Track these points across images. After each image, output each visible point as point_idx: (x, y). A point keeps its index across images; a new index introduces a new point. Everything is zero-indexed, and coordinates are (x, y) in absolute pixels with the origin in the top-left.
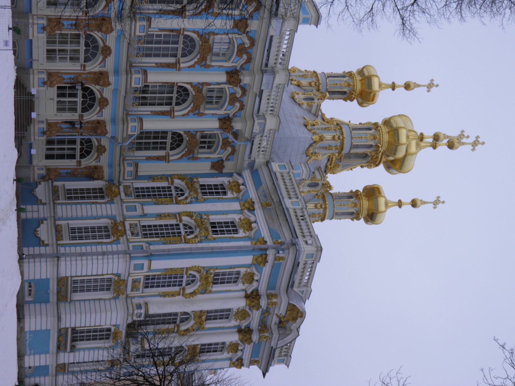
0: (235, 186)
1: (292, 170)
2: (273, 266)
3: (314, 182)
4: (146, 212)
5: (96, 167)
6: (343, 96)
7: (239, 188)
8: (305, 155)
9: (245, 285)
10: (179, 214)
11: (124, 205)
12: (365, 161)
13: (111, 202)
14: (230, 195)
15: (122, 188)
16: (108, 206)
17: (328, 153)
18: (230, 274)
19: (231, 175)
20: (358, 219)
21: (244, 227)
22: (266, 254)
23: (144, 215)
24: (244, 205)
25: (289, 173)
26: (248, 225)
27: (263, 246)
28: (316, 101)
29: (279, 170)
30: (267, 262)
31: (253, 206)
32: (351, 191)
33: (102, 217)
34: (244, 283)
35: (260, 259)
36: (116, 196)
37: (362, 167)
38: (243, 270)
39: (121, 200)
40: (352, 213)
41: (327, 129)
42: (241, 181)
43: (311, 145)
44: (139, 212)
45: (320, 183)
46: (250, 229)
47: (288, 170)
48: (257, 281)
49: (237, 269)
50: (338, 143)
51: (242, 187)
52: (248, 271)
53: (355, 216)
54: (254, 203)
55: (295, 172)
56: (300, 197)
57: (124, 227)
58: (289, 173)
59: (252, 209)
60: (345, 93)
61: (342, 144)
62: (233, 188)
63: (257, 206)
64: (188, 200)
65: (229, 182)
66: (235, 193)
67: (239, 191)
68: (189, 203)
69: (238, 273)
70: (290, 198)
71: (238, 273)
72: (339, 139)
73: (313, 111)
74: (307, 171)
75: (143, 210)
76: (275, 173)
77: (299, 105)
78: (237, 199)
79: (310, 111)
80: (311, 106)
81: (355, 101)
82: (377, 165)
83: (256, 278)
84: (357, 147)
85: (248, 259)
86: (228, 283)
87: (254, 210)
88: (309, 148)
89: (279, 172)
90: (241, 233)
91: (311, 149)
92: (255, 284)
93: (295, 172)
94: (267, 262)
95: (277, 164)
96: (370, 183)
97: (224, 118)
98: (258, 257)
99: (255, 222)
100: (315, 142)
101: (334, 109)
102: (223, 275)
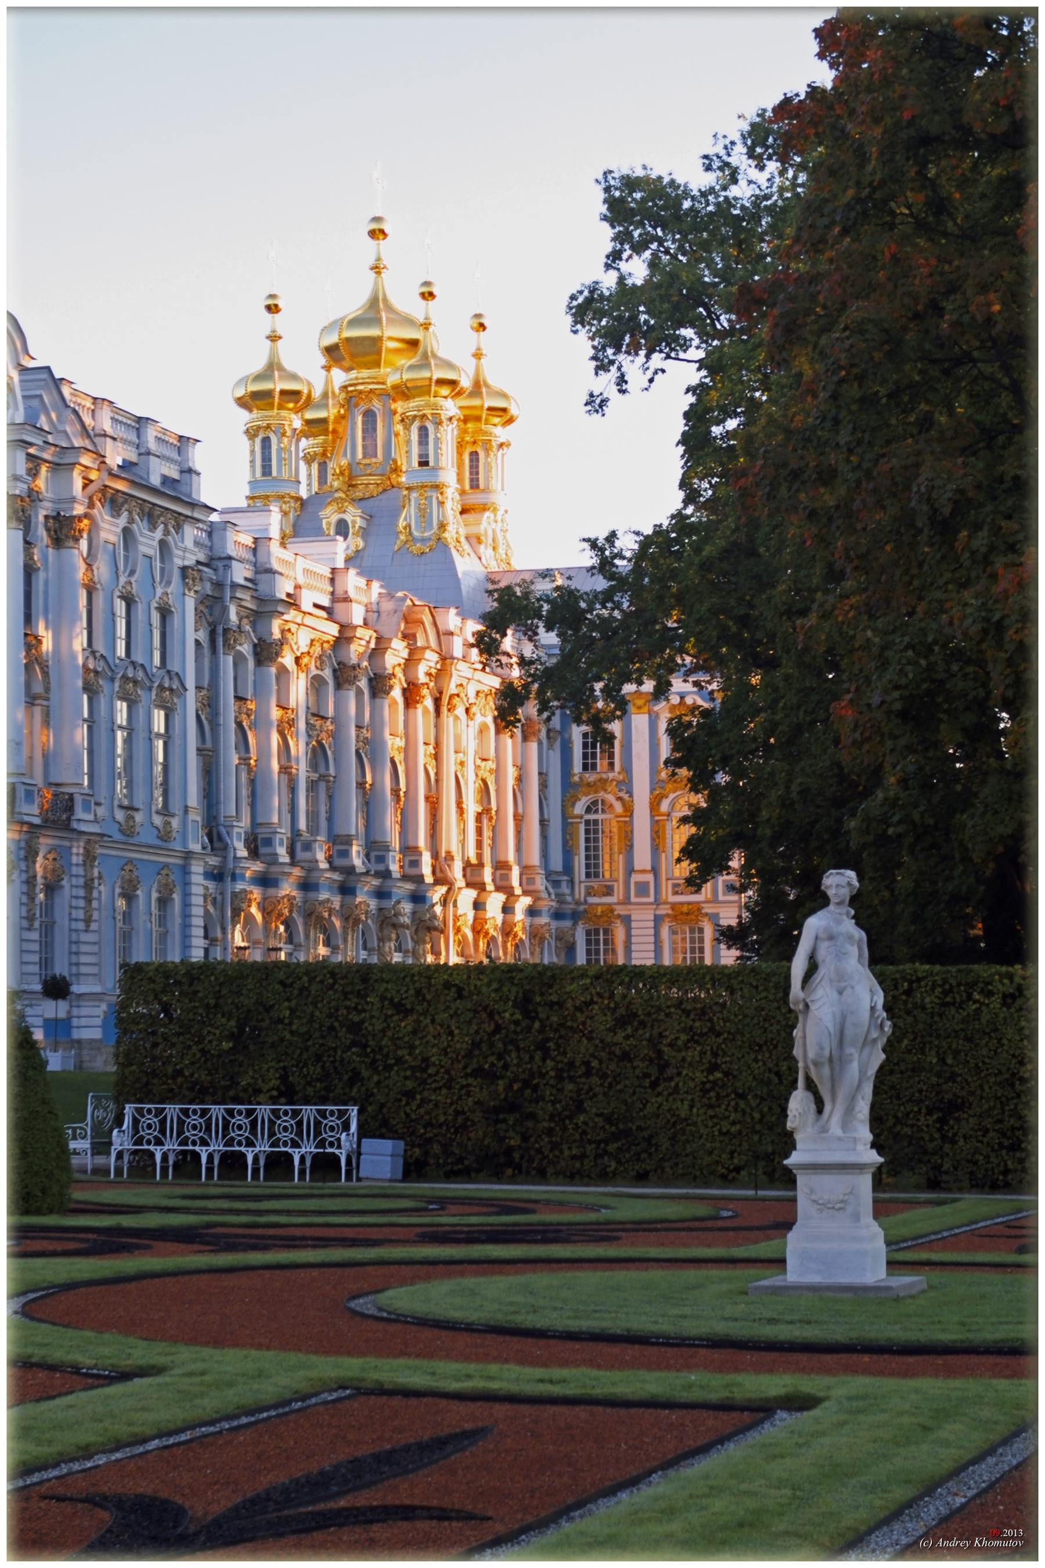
4: (649, 868)
5: (558, 938)
10: (652, 816)
11: (633, 899)
13: (627, 920)
15: (592, 900)
16: (633, 924)
23: (655, 870)
24: (639, 708)
33: (657, 935)
36: (612, 911)
39: (619, 904)
44: (650, 878)
57: (682, 904)
64: (626, 797)
68: (631, 796)
75: (643, 871)
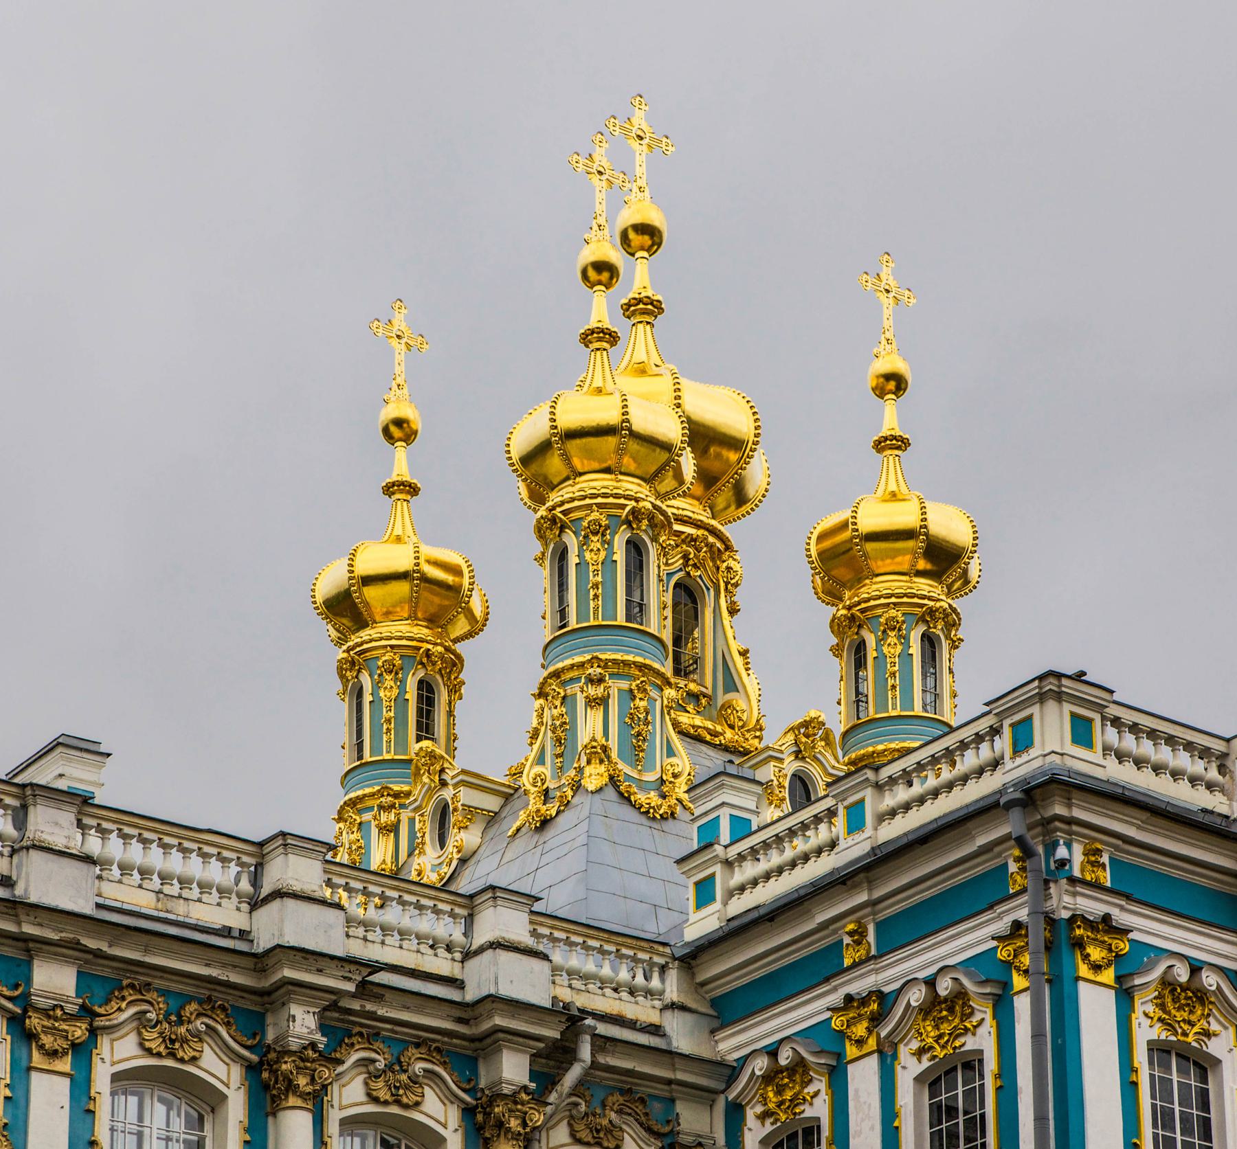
0: (780, 1091)
1: (718, 849)
2: (1128, 897)
3: (787, 784)
6: (443, 696)
7: (791, 1070)
8: (670, 825)
9: (1215, 1027)
12: (710, 598)
14: (820, 1109)
17: (661, 731)
18: (1161, 1088)
19: (735, 1113)
20: (951, 620)
21: (955, 1035)
22: (1072, 920)
24: (860, 1042)
25: (728, 864)
26: (945, 1006)
27: (1037, 935)
28: (448, 793)
29: (717, 906)
30: (1107, 918)
31: (864, 1002)
32: (836, 651)
34: (1207, 1034)
35: (1096, 953)
37: (733, 611)
38: (1145, 1031)
40: (929, 641)
41: (564, 735)
42: (760, 1065)
43: (626, 798)
45: (791, 766)
46: (958, 1002)
47: (717, 869)
48: (1195, 969)
49: (1141, 1057)
50: (616, 687)
51: (784, 1058)
52: (1150, 1008)
53: (937, 633)
54: (849, 999)
55: (725, 837)
56: (828, 803)
58: (728, 864)
59: (874, 1006)
60: (426, 691)
61: (621, 669)
62: (788, 1095)
63: (859, 985)
65: (763, 1117)
66: (811, 1089)
67: (799, 1068)
69: (1159, 1050)
70: (833, 844)
71: (1159, 1050)
72: (601, 680)
73: (491, 803)
74: (722, 786)
76: (729, 920)
77: (463, 861)
78: (837, 1075)
79: (492, 819)
80: (470, 811)
81: (458, 647)
82: (728, 548)
83: (1182, 974)
84: (637, 609)
85: (1095, 1006)
86: (1205, 1105)
87: (880, 995)
88: (637, 807)
89: (725, 904)
90: (984, 1040)
91: (641, 797)
92: (1210, 980)
93: (725, 837)
94: (1107, 918)
95: (693, 917)
96: (802, 578)
97: (479, 1129)
98: (1086, 957)
99: (931, 983)
100: (613, 780)
101: (495, 724)
102: (1168, 1123)
